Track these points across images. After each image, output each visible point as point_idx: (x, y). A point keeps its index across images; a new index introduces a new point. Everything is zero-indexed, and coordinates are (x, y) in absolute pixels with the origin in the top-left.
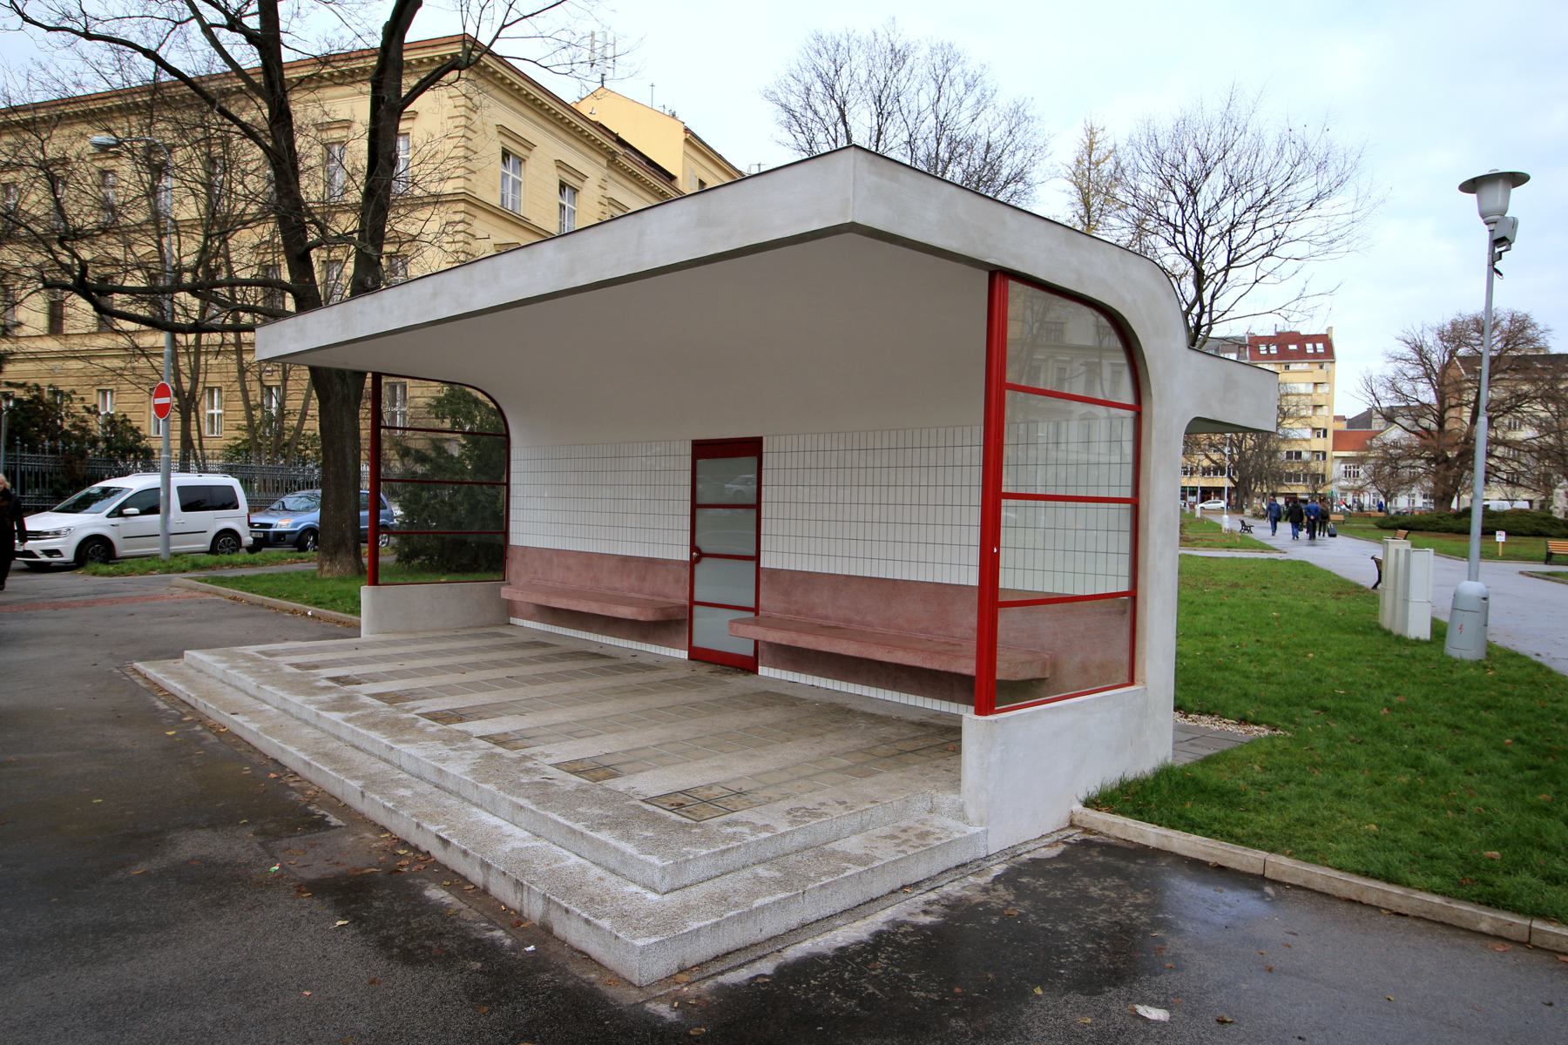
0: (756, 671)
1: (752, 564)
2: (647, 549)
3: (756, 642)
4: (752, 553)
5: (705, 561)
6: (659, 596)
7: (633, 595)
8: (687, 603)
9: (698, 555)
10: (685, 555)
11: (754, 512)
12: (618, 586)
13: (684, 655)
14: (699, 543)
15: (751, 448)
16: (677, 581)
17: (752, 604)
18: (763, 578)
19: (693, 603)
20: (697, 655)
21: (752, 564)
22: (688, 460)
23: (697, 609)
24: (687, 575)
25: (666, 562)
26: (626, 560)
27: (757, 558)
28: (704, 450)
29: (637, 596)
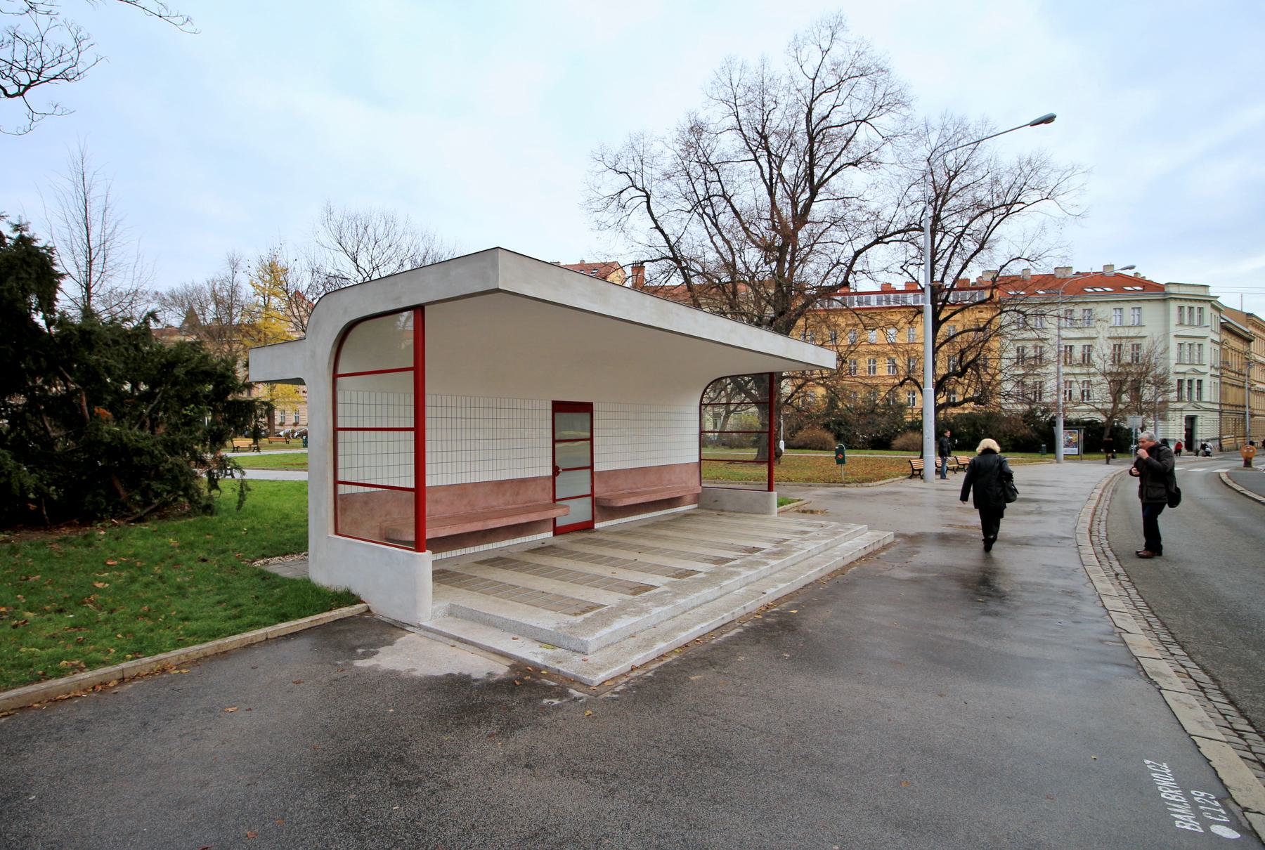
0: (593, 527)
1: (588, 471)
2: (541, 471)
4: (588, 464)
6: (530, 502)
7: (510, 507)
9: (556, 470)
10: (550, 473)
12: (495, 503)
13: (550, 534)
15: (587, 408)
16: (543, 490)
18: (595, 477)
20: (557, 531)
21: (588, 471)
22: (550, 413)
25: (534, 479)
26: (500, 484)
27: (592, 467)
28: (558, 407)
29: (513, 506)
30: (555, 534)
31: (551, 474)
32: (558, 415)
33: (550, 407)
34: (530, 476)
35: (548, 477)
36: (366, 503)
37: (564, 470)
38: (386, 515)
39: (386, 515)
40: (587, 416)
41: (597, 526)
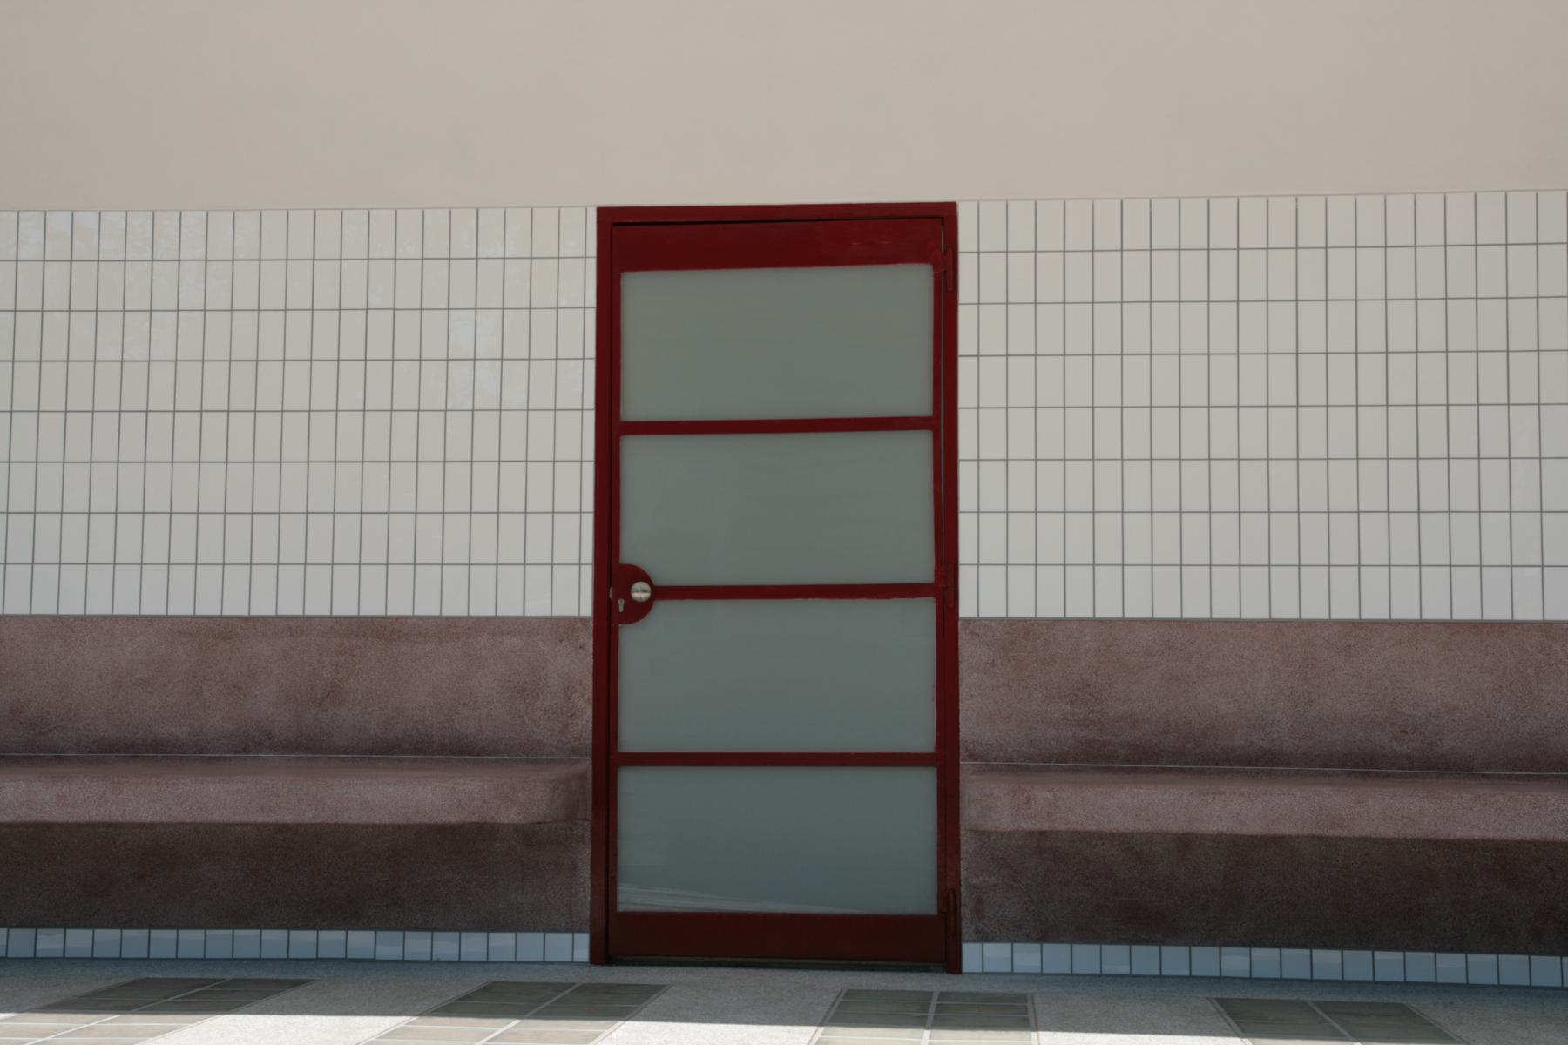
0: (953, 964)
1: (924, 611)
4: (923, 570)
5: (664, 610)
11: (920, 444)
13: (579, 946)
14: (631, 551)
18: (969, 652)
23: (631, 782)
24: (582, 666)
27: (944, 587)
30: (602, 954)
31: (587, 610)
33: (583, 241)
34: (427, 607)
35: (560, 627)
37: (662, 593)
40: (916, 280)
41: (973, 955)
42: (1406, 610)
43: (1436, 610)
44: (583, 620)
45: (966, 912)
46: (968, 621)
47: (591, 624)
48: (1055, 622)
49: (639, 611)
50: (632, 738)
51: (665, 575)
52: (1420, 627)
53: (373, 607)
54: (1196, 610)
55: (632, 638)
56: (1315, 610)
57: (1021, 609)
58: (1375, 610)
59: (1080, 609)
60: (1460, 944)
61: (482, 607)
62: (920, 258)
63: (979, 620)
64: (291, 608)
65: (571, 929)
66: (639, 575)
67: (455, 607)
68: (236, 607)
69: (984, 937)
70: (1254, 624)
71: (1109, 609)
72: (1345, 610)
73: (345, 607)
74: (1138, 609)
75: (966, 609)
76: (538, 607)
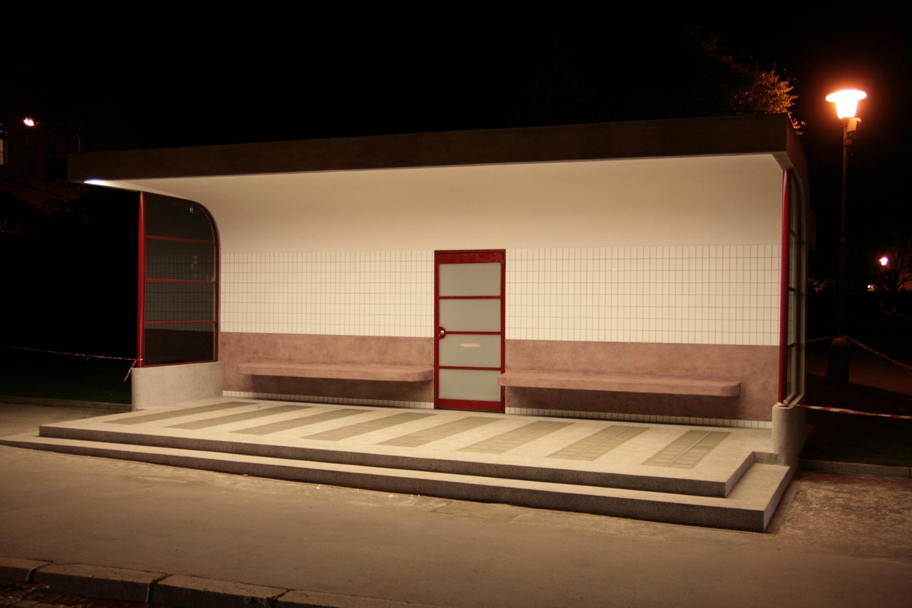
1: (499, 338)
3: (503, 388)
4: (498, 329)
5: (448, 337)
8: (432, 368)
9: (440, 333)
10: (431, 333)
11: (498, 302)
13: (432, 405)
14: (442, 324)
17: (499, 365)
18: (507, 346)
19: (437, 367)
23: (442, 373)
24: (432, 348)
27: (502, 333)
28: (443, 258)
31: (433, 336)
32: (443, 268)
35: (427, 340)
36: (239, 341)
37: (447, 333)
38: (254, 353)
39: (254, 353)
40: (497, 266)
41: (507, 410)
42: (596, 340)
43: (602, 340)
44: (432, 338)
45: (506, 401)
46: (507, 340)
47: (434, 339)
48: (524, 340)
49: (443, 336)
50: (442, 363)
51: (448, 330)
52: (599, 343)
53: (392, 335)
54: (553, 339)
55: (442, 343)
56: (577, 339)
57: (518, 338)
58: (589, 340)
59: (529, 338)
60: (605, 411)
61: (413, 335)
62: (499, 262)
63: (509, 340)
64: (377, 334)
65: (430, 402)
66: (443, 329)
67: (408, 335)
68: (367, 334)
69: (510, 406)
70: (564, 342)
71: (535, 338)
72: (583, 339)
73: (387, 335)
74: (541, 338)
75: (507, 337)
76: (424, 335)
